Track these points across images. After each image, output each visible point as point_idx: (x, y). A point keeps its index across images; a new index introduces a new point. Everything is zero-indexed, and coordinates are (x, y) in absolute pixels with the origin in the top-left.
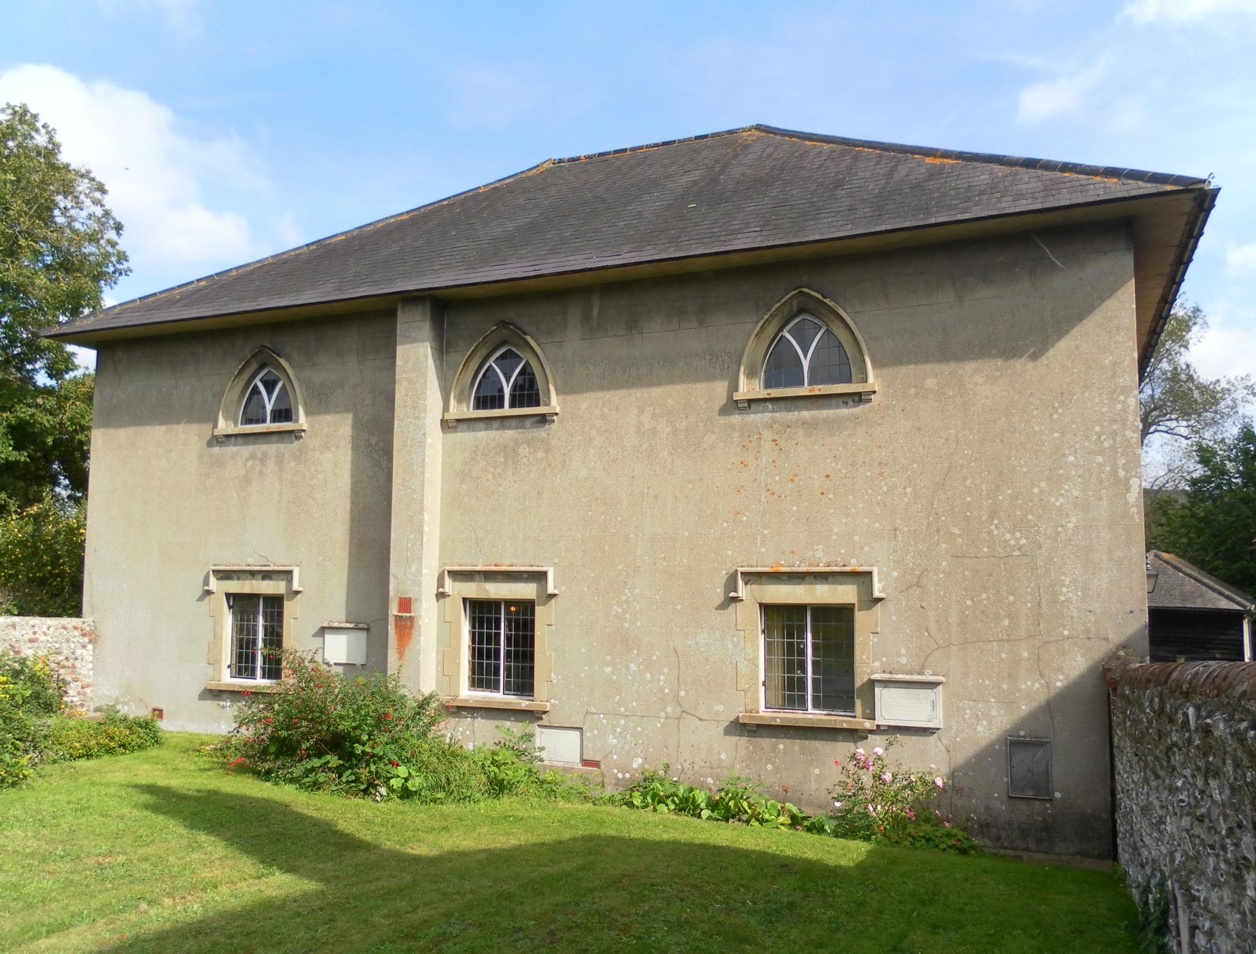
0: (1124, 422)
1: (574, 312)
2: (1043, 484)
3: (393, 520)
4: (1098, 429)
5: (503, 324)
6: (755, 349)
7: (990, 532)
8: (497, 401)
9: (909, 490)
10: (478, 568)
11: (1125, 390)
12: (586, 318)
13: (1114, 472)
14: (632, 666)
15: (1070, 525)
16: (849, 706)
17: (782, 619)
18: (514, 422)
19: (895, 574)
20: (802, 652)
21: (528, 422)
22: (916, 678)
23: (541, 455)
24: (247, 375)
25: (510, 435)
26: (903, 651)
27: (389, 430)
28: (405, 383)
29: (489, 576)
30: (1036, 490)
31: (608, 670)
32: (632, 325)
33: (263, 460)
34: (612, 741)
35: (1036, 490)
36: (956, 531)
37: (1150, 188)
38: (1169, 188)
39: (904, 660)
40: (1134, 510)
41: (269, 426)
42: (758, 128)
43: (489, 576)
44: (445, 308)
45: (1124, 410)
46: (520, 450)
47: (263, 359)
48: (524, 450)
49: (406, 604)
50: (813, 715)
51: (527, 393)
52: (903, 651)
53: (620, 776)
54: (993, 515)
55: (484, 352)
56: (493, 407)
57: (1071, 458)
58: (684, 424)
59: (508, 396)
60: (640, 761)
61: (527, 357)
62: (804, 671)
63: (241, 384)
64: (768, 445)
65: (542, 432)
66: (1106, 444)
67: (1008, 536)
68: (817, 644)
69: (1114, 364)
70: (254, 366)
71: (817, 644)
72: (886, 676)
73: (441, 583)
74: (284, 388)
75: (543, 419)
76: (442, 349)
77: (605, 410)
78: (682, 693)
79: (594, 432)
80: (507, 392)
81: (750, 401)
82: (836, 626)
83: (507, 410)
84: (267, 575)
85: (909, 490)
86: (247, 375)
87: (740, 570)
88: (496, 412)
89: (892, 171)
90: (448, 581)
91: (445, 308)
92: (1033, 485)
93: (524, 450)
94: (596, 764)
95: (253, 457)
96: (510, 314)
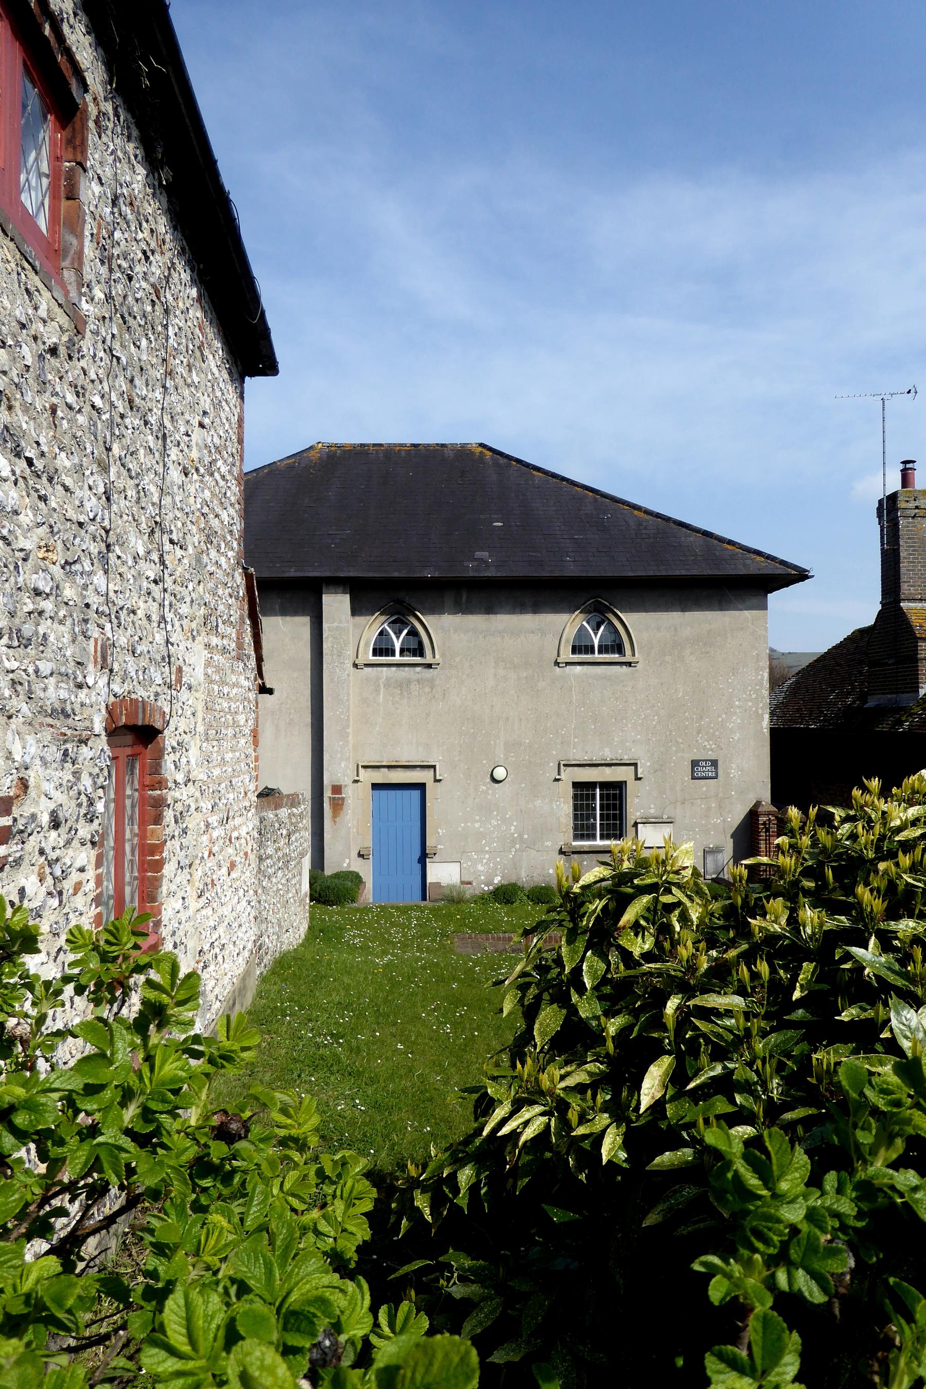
0: (762, 684)
2: (724, 716)
3: (325, 733)
4: (750, 688)
7: (697, 741)
8: (390, 652)
9: (656, 717)
10: (384, 764)
11: (762, 669)
13: (756, 711)
14: (493, 821)
15: (736, 738)
16: (620, 836)
17: (582, 789)
19: (648, 764)
20: (594, 809)
22: (660, 820)
23: (427, 689)
26: (652, 806)
28: (330, 639)
30: (720, 719)
31: (477, 825)
34: (480, 867)
35: (720, 719)
36: (680, 740)
38: (793, 572)
39: (652, 811)
40: (765, 730)
45: (762, 679)
46: (413, 685)
49: (337, 789)
50: (599, 843)
52: (652, 806)
53: (486, 888)
54: (699, 732)
56: (387, 655)
57: (737, 703)
58: (525, 674)
60: (499, 878)
62: (595, 819)
66: (754, 696)
67: (706, 743)
68: (602, 805)
69: (758, 655)
71: (602, 805)
72: (644, 820)
75: (429, 666)
76: (355, 612)
77: (473, 663)
78: (526, 836)
79: (465, 677)
80: (398, 646)
82: (615, 793)
83: (397, 658)
85: (656, 717)
87: (562, 763)
88: (389, 659)
90: (361, 770)
92: (719, 716)
93: (414, 687)
94: (470, 883)
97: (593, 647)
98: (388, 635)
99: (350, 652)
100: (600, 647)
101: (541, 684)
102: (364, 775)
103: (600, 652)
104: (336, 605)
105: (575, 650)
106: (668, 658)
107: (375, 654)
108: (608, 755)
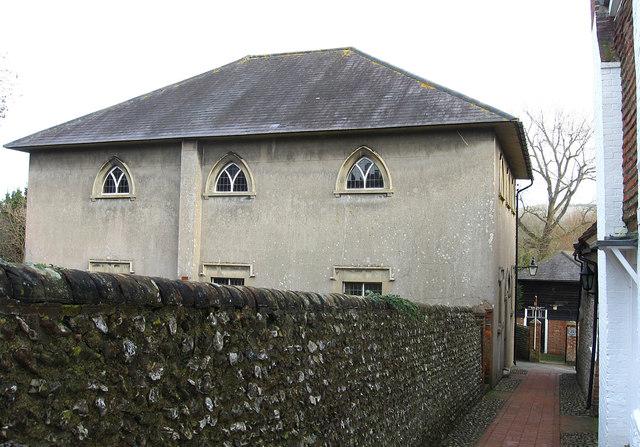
1: (264, 150)
5: (231, 153)
6: (343, 172)
12: (269, 153)
18: (235, 199)
21: (242, 199)
24: (106, 170)
25: (234, 202)
27: (178, 199)
29: (223, 267)
32: (290, 157)
33: (115, 210)
37: (498, 118)
38: (505, 120)
41: (116, 194)
42: (351, 49)
43: (223, 267)
44: (204, 144)
47: (114, 162)
48: (240, 211)
51: (242, 184)
55: (222, 165)
59: (234, 183)
61: (241, 168)
63: (104, 174)
64: (348, 214)
65: (248, 203)
70: (110, 166)
73: (201, 270)
74: (124, 177)
75: (249, 197)
76: (203, 162)
81: (341, 194)
84: (117, 265)
86: (106, 170)
89: (407, 89)
91: (204, 144)
93: (240, 211)
95: (109, 209)
96: (234, 149)
97: (362, 182)
98: (226, 175)
99: (198, 186)
100: (367, 182)
101: (323, 210)
102: (205, 271)
103: (367, 187)
104: (190, 157)
105: (350, 185)
106: (415, 190)
107: (218, 190)
108: (368, 262)
